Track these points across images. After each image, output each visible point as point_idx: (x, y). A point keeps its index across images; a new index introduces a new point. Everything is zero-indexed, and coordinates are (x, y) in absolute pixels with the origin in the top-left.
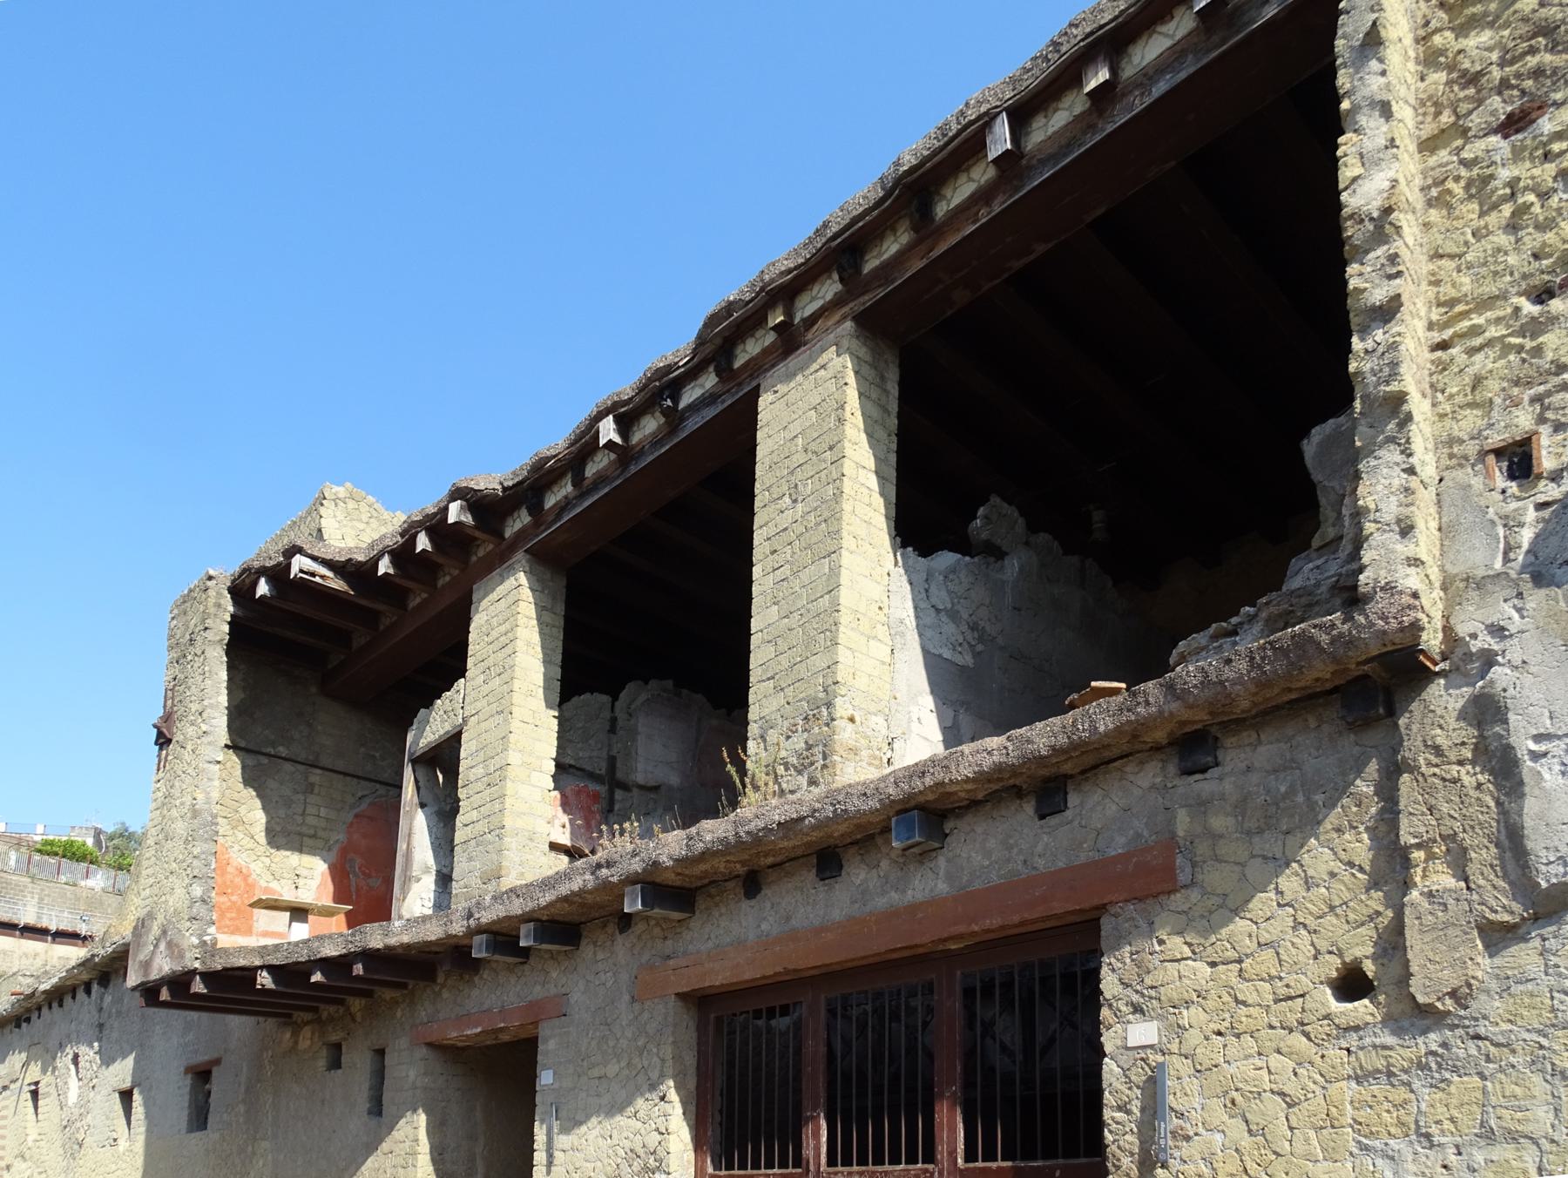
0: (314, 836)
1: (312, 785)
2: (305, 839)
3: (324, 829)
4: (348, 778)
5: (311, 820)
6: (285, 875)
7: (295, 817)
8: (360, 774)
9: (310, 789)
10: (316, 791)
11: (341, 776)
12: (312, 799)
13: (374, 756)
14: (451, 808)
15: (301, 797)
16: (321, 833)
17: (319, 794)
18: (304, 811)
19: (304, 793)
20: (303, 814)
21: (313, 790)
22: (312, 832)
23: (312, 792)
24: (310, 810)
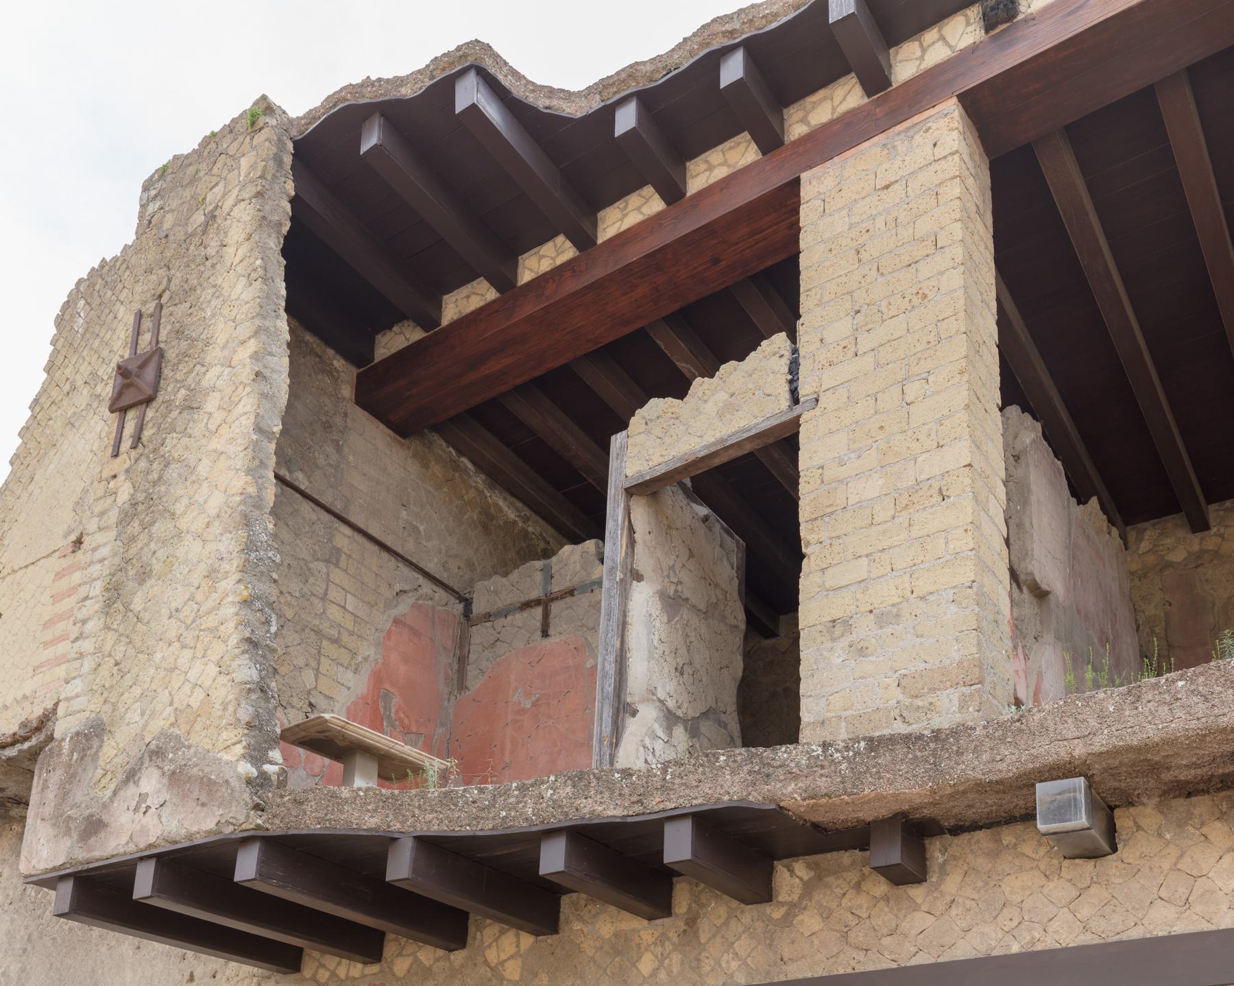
0: (336, 641)
1: (338, 551)
2: (325, 643)
3: (351, 634)
4: (385, 555)
5: (334, 612)
6: (295, 701)
7: (313, 599)
8: (400, 551)
9: (333, 557)
10: (343, 564)
11: (376, 548)
12: (337, 576)
13: (415, 529)
14: (676, 591)
15: (321, 566)
16: (345, 638)
17: (346, 571)
18: (326, 594)
19: (327, 561)
20: (324, 598)
21: (338, 560)
22: (334, 633)
23: (337, 565)
24: (334, 594)
